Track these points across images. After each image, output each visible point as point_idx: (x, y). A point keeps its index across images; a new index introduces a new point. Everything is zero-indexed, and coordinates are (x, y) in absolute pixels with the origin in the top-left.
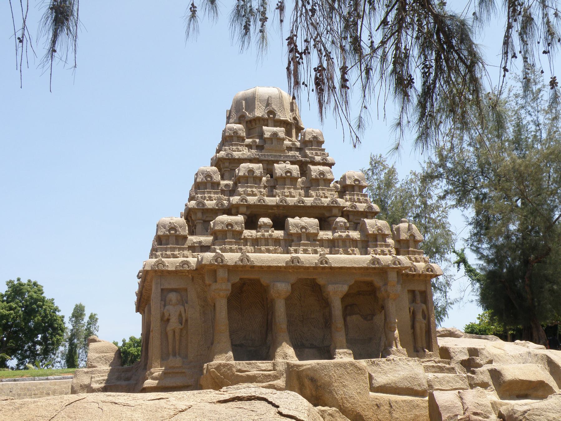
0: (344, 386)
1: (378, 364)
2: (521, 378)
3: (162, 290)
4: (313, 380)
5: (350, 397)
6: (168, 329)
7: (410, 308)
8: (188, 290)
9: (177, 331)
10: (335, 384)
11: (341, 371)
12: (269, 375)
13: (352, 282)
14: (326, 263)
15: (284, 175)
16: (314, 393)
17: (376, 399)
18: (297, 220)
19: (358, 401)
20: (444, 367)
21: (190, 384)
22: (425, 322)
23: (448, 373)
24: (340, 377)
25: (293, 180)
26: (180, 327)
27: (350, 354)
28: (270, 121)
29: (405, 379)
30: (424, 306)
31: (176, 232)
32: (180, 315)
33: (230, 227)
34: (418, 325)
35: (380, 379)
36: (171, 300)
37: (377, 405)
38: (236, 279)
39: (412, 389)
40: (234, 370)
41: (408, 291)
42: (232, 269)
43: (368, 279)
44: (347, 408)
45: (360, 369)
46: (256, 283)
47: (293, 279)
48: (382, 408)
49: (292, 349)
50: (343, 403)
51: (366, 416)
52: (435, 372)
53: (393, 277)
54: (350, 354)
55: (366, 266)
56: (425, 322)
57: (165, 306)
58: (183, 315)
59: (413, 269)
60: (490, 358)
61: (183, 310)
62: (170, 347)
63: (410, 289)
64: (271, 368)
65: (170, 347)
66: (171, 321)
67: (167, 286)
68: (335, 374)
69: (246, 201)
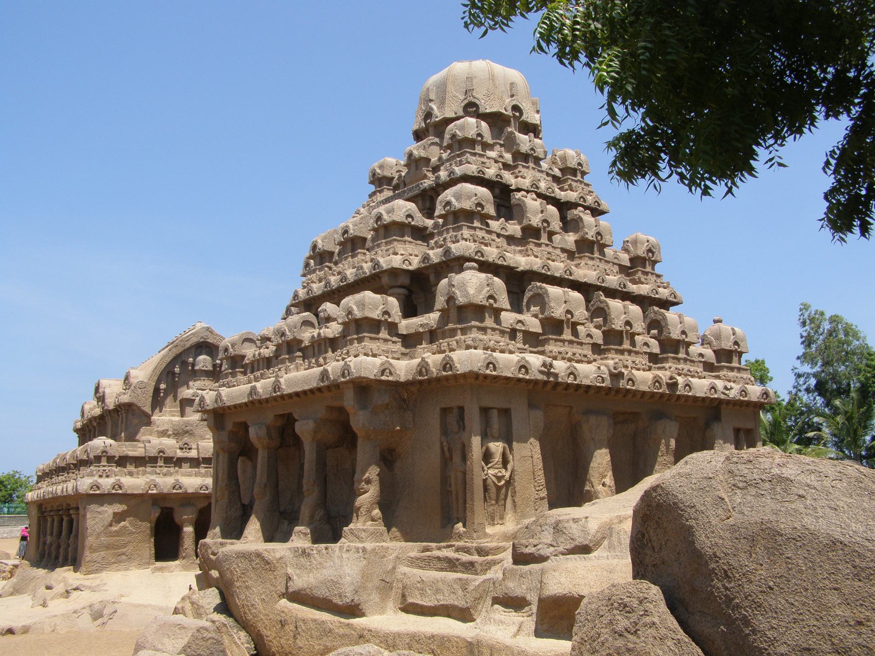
0: (247, 587)
1: (309, 555)
5: (253, 605)
7: (442, 443)
10: (238, 584)
11: (244, 564)
17: (283, 612)
19: (260, 612)
20: (458, 560)
23: (463, 572)
24: (243, 574)
27: (305, 534)
29: (324, 583)
35: (301, 581)
37: (281, 621)
38: (229, 426)
40: (210, 552)
41: (445, 411)
44: (249, 621)
45: (269, 563)
47: (269, 417)
48: (287, 627)
49: (258, 524)
50: (245, 613)
51: (267, 636)
52: (442, 570)
54: (305, 534)
55: (315, 385)
59: (424, 370)
60: (580, 541)
63: (443, 406)
68: (237, 568)
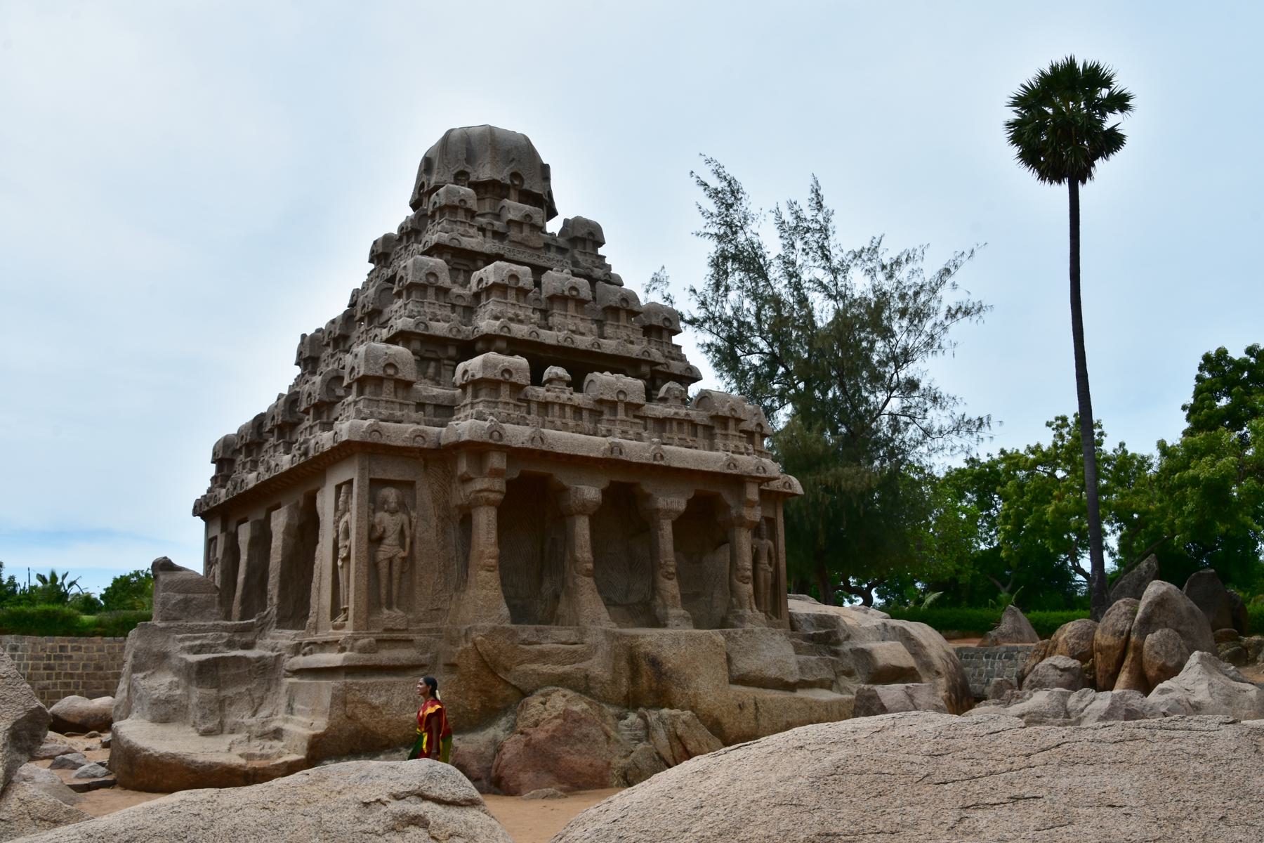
2: (894, 662)
3: (371, 480)
4: (655, 663)
6: (381, 556)
8: (418, 486)
9: (397, 562)
12: (575, 651)
13: (691, 495)
14: (662, 457)
15: (566, 293)
16: (654, 685)
18: (607, 376)
21: (423, 662)
22: (771, 569)
25: (580, 303)
26: (403, 554)
28: (512, 192)
30: (771, 543)
31: (397, 372)
32: (402, 532)
33: (507, 376)
34: (762, 574)
36: (385, 502)
39: (782, 680)
42: (514, 454)
43: (712, 489)
46: (544, 480)
47: (604, 483)
53: (752, 493)
56: (771, 569)
57: (374, 512)
58: (407, 533)
61: (406, 522)
62: (383, 592)
64: (573, 639)
65: (383, 592)
66: (386, 541)
67: (380, 475)
69: (509, 330)
